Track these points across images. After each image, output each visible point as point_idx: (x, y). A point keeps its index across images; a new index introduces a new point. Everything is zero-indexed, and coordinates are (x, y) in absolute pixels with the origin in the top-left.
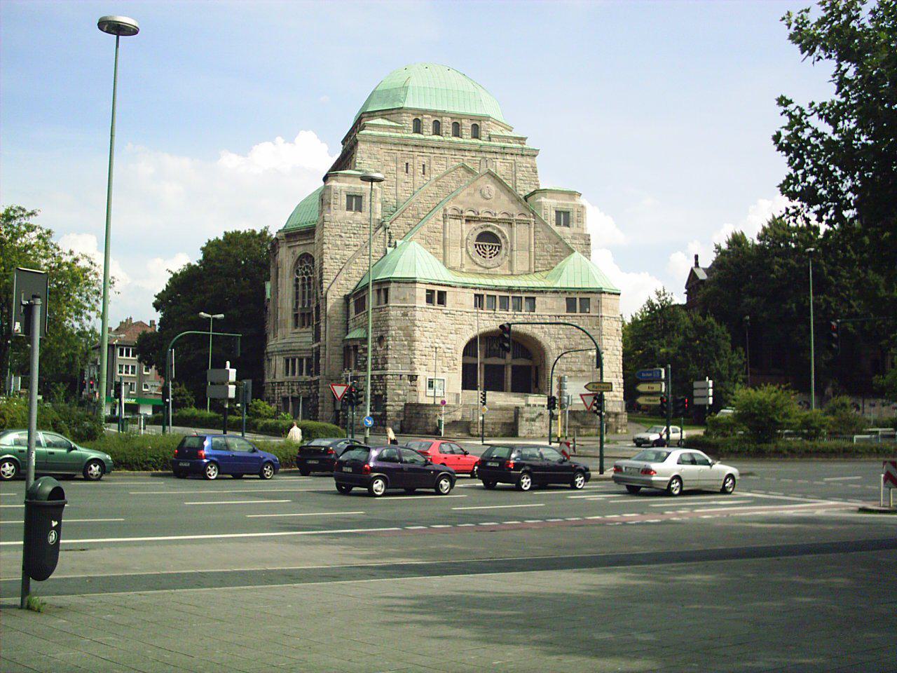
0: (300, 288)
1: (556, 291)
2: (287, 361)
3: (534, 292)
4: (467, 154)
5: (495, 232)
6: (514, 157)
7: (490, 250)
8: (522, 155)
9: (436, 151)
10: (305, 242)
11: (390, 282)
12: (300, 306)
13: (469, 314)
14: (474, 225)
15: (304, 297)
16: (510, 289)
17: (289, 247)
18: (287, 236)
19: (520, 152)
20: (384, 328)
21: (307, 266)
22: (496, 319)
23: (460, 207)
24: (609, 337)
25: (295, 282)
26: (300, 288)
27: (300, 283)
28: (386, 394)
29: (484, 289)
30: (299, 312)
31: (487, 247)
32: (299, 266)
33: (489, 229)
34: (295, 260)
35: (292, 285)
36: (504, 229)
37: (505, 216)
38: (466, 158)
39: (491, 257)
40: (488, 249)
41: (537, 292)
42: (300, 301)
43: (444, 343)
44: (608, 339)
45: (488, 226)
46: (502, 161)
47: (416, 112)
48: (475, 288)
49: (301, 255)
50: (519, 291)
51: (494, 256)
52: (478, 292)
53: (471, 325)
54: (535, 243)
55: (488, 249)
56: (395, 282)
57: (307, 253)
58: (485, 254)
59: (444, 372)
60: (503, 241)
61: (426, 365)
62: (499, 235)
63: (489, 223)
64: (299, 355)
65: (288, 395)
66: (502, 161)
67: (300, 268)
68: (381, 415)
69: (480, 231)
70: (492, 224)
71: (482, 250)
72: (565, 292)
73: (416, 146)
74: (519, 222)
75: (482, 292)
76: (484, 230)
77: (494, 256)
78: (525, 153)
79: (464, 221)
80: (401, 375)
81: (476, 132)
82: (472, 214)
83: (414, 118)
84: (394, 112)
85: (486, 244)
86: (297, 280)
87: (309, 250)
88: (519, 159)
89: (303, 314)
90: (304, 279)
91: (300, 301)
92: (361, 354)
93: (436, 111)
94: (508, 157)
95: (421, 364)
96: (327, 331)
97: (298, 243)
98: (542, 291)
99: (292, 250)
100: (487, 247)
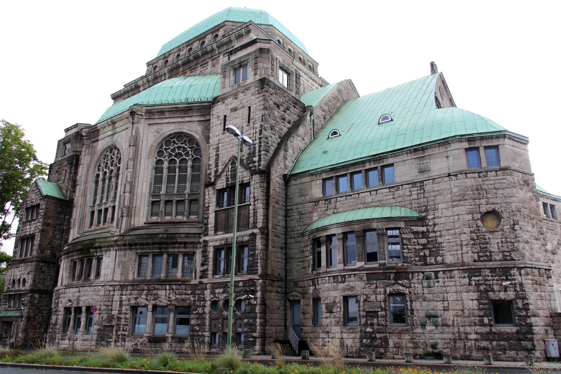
0: (165, 171)
2: (141, 256)
10: (180, 120)
11: (504, 136)
12: (163, 191)
15: (171, 180)
17: (149, 124)
18: (149, 112)
20: (499, 201)
21: (179, 148)
25: (155, 165)
26: (165, 171)
27: (166, 164)
28: (524, 298)
30: (163, 198)
32: (164, 147)
34: (160, 140)
35: (150, 167)
42: (164, 186)
49: (170, 135)
56: (509, 138)
57: (182, 133)
64: (170, 250)
65: (147, 303)
67: (165, 149)
68: (518, 332)
80: (540, 269)
84: (261, 27)
86: (159, 162)
87: (193, 128)
89: (167, 202)
90: (172, 161)
91: (164, 186)
92: (409, 239)
96: (271, 215)
97: (167, 121)
99: (155, 128)
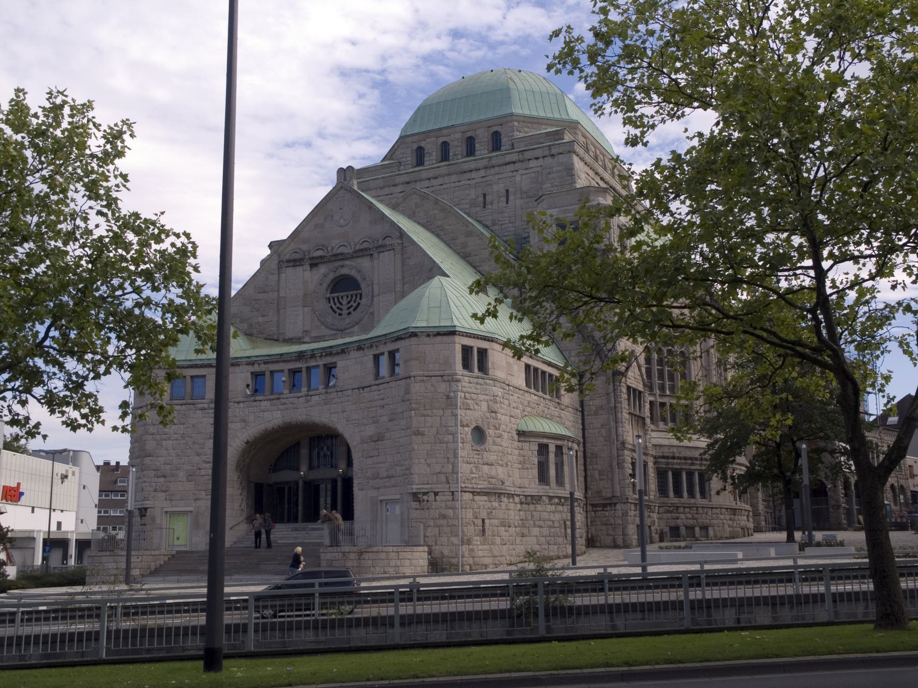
1: (360, 347)
3: (331, 354)
4: (474, 175)
5: (353, 273)
6: (540, 162)
7: (349, 303)
8: (553, 156)
9: (434, 182)
13: (241, 405)
14: (323, 269)
16: (301, 356)
19: (547, 153)
22: (281, 407)
23: (305, 247)
24: (429, 412)
29: (265, 363)
31: (345, 298)
33: (344, 271)
36: (365, 263)
37: (365, 245)
38: (474, 181)
39: (349, 313)
40: (344, 302)
41: (338, 354)
43: (198, 455)
44: (424, 415)
45: (342, 266)
46: (524, 172)
47: (416, 138)
48: (253, 364)
50: (313, 356)
51: (354, 310)
52: (256, 368)
53: (244, 421)
54: (403, 278)
55: (344, 302)
58: (341, 310)
59: (198, 499)
60: (363, 285)
61: (165, 491)
62: (359, 278)
63: (341, 263)
66: (524, 172)
69: (331, 276)
70: (347, 263)
71: (338, 305)
72: (372, 346)
73: (408, 183)
74: (381, 248)
75: (263, 368)
76: (337, 274)
77: (354, 310)
78: (554, 151)
79: (308, 267)
81: (496, 142)
82: (319, 253)
83: (415, 146)
85: (342, 294)
88: (549, 160)
93: (441, 129)
94: (533, 164)
95: (155, 491)
98: (343, 350)
100: (345, 298)
